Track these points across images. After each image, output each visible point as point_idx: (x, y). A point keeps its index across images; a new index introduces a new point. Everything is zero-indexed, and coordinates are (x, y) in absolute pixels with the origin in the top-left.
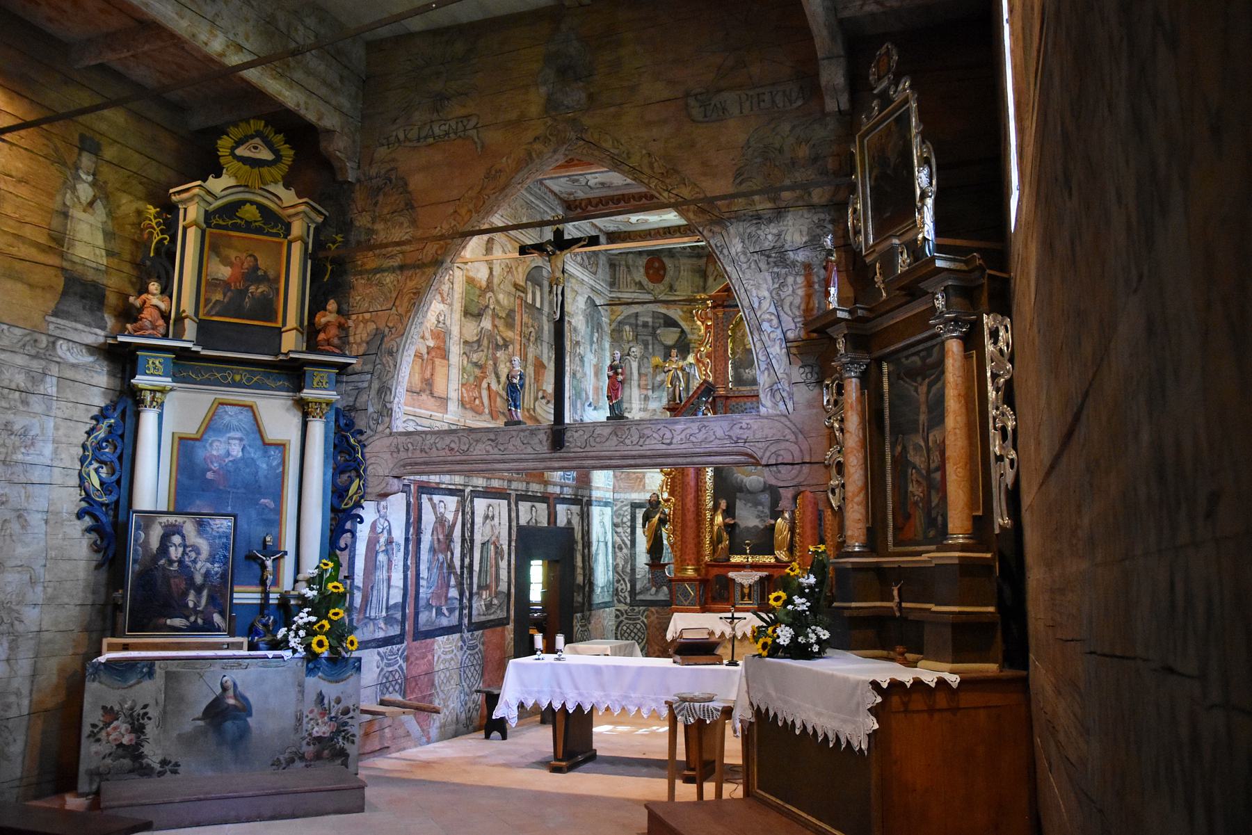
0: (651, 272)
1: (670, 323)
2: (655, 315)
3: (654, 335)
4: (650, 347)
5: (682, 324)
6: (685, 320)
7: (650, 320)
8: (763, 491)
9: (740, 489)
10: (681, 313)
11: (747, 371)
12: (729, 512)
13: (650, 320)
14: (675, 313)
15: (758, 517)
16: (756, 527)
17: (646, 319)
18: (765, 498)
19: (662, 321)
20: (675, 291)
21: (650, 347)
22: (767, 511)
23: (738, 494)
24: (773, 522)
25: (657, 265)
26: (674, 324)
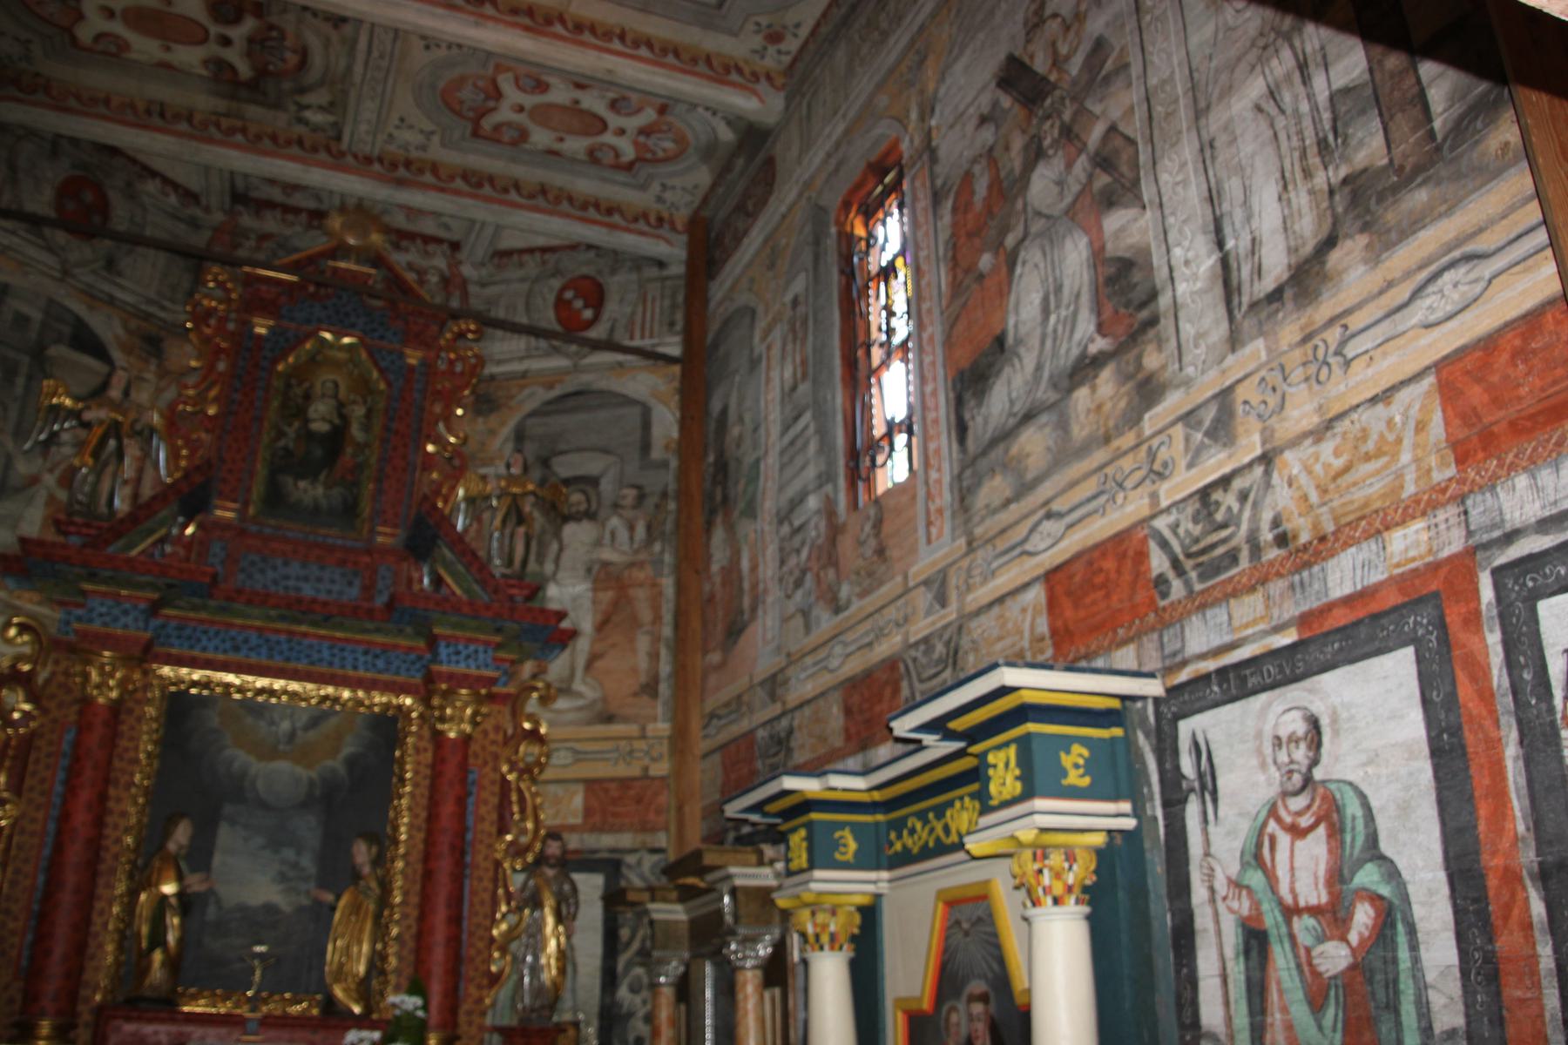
0: (71, 206)
1: (87, 342)
2: (53, 309)
3: (38, 354)
4: (20, 381)
5: (117, 355)
6: (128, 350)
7: (36, 316)
8: (305, 805)
9: (238, 789)
10: (120, 332)
11: (302, 484)
12: (199, 856)
13: (36, 316)
14: (107, 327)
15: (282, 878)
16: (270, 909)
17: (25, 309)
18: (308, 827)
19: (67, 330)
20: (120, 274)
21: (20, 381)
22: (307, 862)
23: (228, 809)
24: (329, 897)
25: (89, 197)
26: (97, 349)
